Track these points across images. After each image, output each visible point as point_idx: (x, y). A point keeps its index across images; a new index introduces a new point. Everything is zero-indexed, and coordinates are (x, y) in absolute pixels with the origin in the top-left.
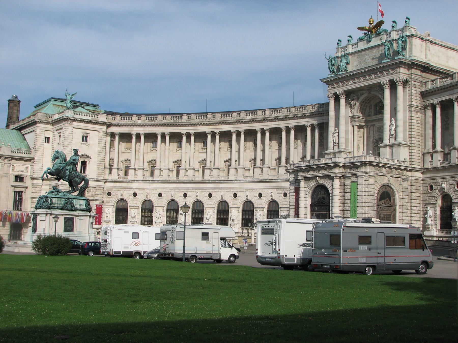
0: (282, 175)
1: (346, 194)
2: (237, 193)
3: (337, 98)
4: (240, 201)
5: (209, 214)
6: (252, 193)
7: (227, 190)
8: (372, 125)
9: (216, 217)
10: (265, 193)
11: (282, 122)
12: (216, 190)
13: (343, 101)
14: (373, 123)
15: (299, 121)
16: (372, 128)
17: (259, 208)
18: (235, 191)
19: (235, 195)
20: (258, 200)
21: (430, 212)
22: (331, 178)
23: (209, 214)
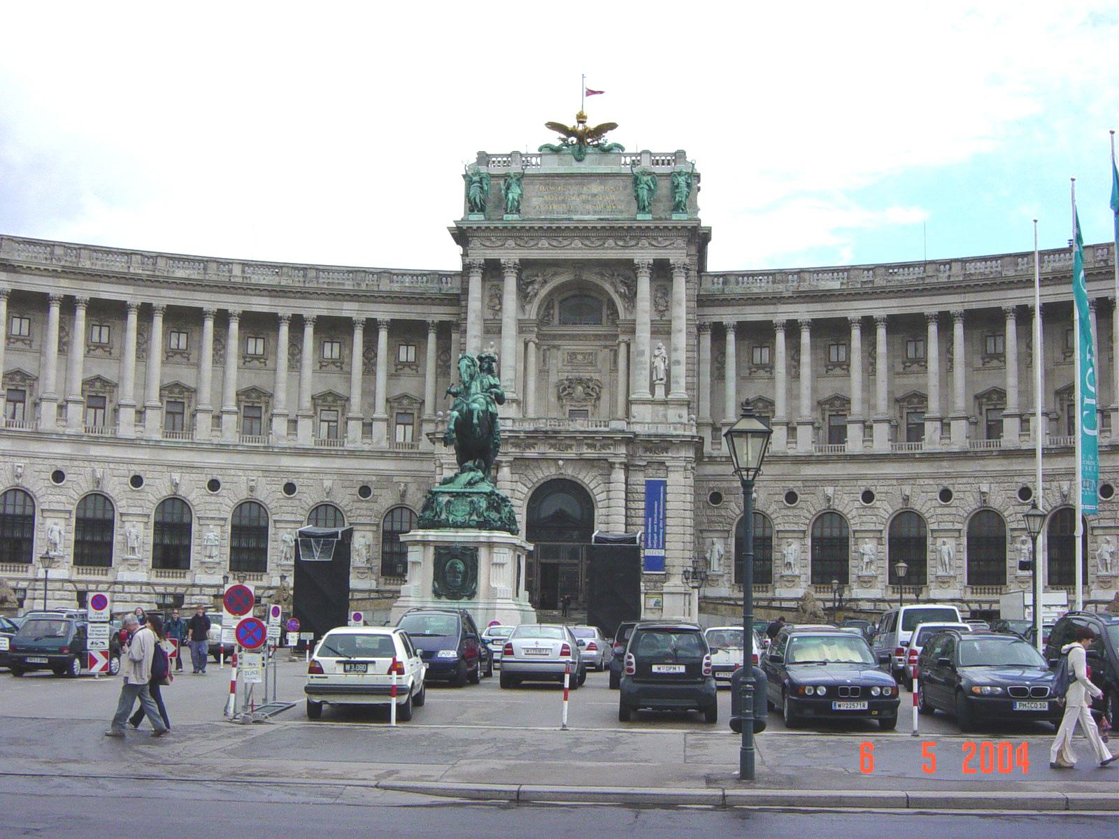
0: (279, 437)
1: (632, 505)
2: (142, 474)
3: (493, 270)
4: (151, 498)
5: (57, 528)
6: (187, 477)
7: (112, 466)
8: (554, 347)
9: (72, 537)
10: (227, 478)
11: (282, 301)
12: (76, 463)
13: (510, 283)
14: (556, 343)
15: (334, 304)
16: (554, 351)
17: (213, 518)
18: (137, 470)
19: (137, 481)
20: (208, 499)
21: (719, 547)
22: (607, 467)
23: (57, 528)
